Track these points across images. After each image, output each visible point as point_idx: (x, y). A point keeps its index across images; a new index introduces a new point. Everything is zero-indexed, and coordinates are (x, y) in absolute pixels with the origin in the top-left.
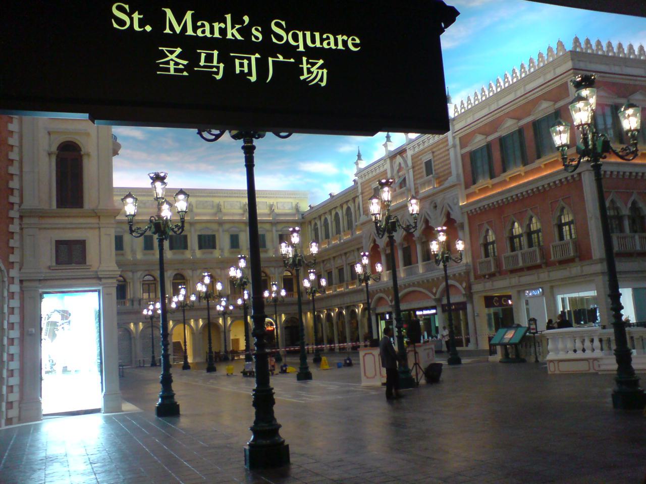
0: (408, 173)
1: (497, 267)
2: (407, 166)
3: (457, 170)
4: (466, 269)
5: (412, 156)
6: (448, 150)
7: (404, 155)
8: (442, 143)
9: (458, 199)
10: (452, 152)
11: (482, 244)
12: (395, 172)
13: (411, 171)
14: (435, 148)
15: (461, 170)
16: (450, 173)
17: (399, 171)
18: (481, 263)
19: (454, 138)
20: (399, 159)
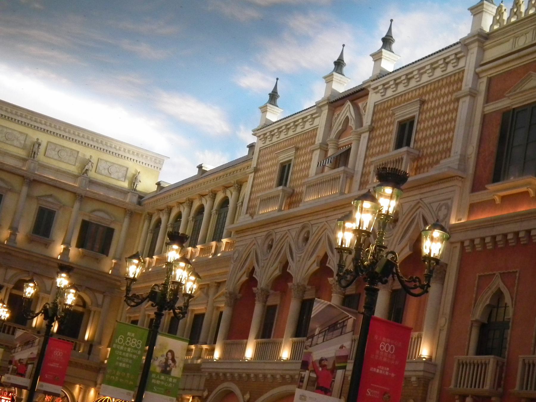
0: (359, 140)
1: (499, 385)
3: (465, 147)
4: (424, 371)
5: (375, 106)
6: (457, 100)
8: (448, 85)
9: (449, 209)
10: (464, 106)
11: (476, 321)
12: (333, 135)
13: (365, 137)
14: (428, 93)
15: (472, 150)
16: (449, 150)
18: (462, 364)
19: (477, 76)
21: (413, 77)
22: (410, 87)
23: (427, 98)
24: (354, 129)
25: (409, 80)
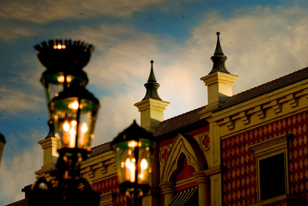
0: (208, 184)
2: (203, 164)
5: (221, 141)
7: (197, 138)
14: (296, 126)
17: (175, 177)
20: (182, 146)
21: (271, 107)
22: (267, 118)
23: (294, 132)
24: (197, 169)
25: (264, 111)
